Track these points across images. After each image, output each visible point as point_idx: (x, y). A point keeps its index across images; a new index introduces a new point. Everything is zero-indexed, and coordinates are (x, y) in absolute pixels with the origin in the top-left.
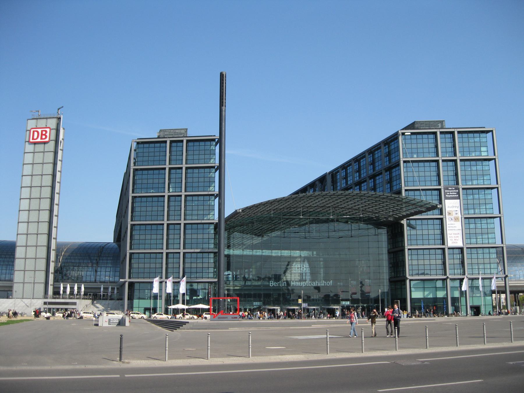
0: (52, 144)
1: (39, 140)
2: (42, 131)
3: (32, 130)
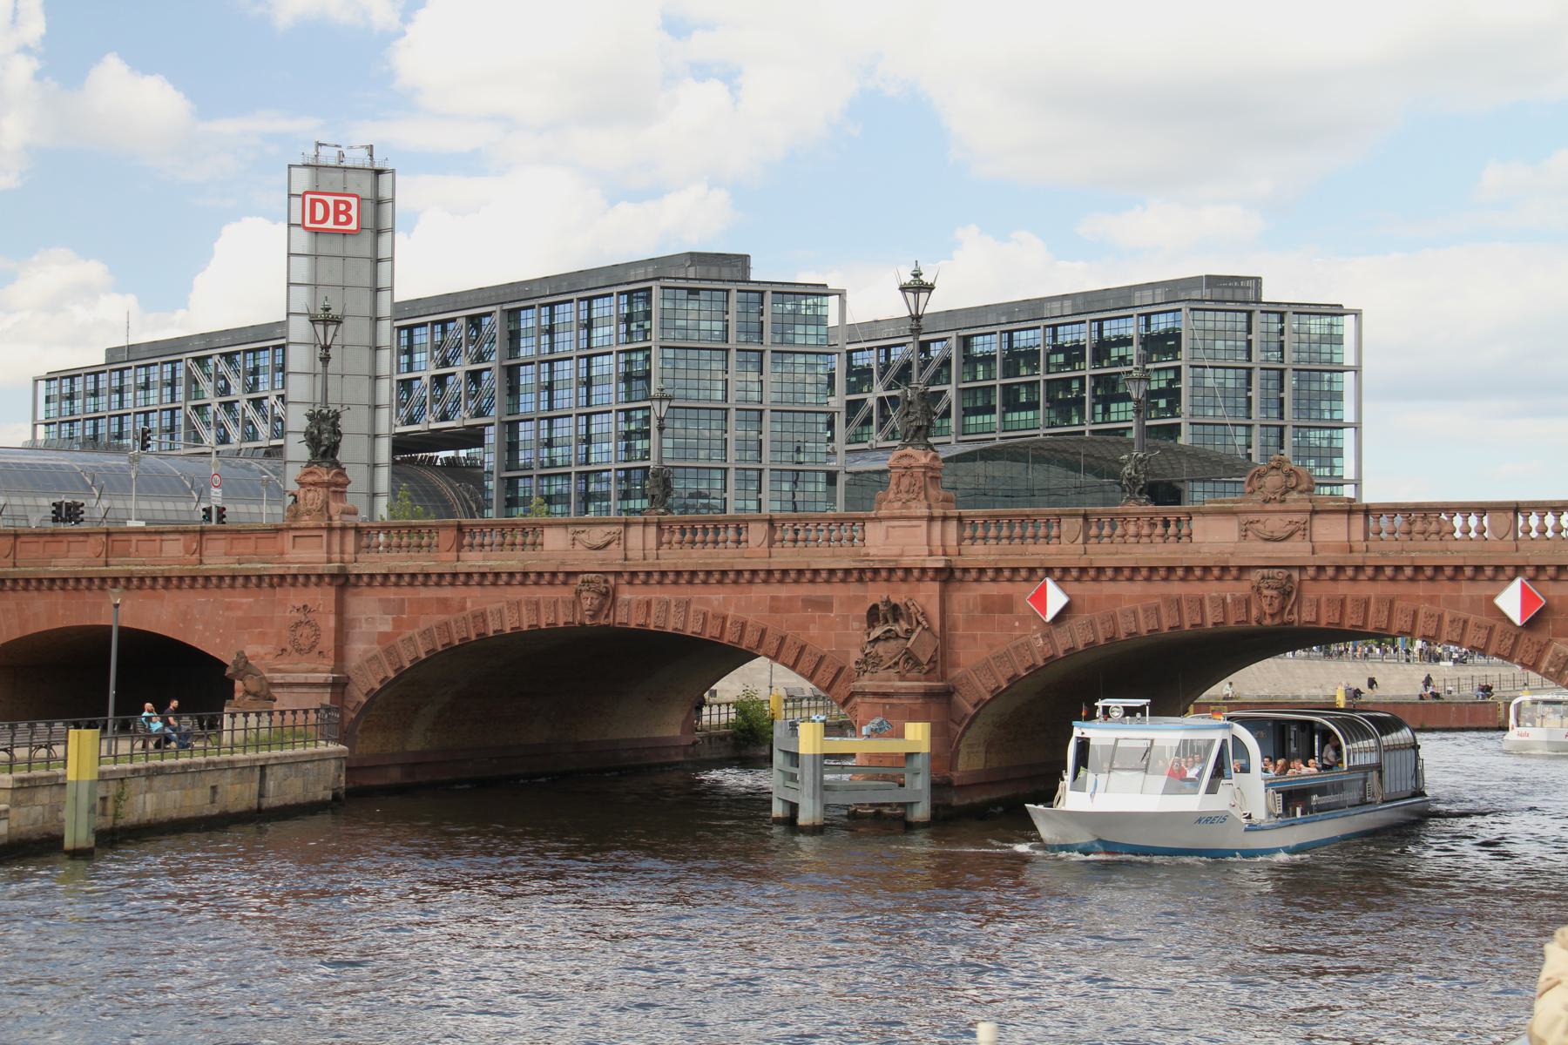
0: (368, 236)
1: (330, 224)
2: (337, 203)
3: (308, 197)
